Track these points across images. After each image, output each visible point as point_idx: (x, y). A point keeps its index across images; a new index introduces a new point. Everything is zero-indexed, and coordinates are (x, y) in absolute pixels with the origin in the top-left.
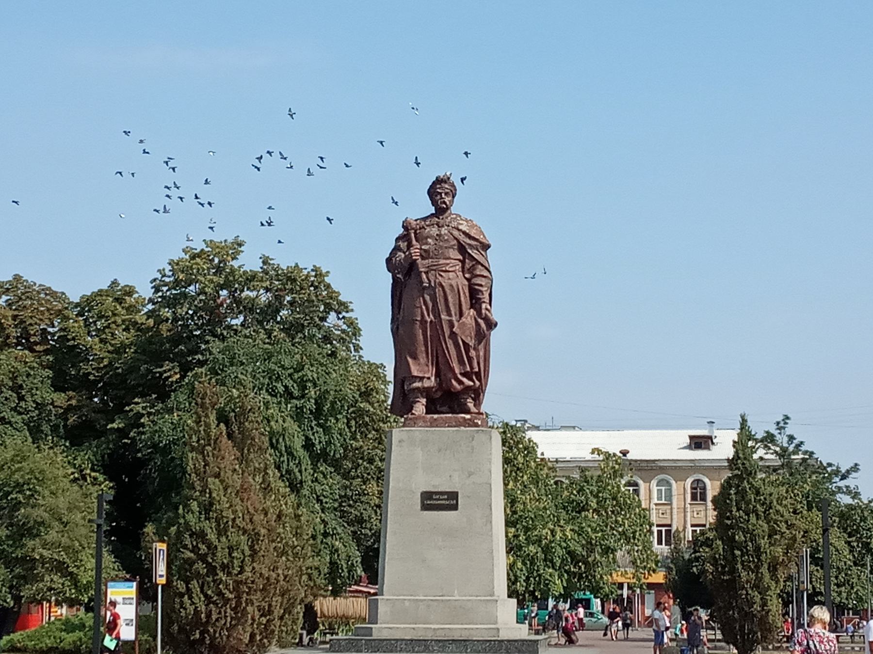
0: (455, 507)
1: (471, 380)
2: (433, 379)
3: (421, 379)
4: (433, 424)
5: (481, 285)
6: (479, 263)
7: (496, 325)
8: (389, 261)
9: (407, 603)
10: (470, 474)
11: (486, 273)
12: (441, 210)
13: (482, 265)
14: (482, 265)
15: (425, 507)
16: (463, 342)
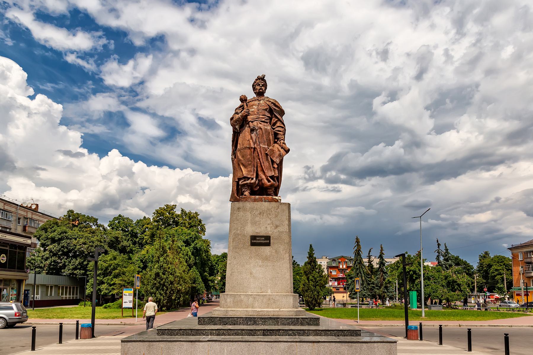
0: (268, 244)
1: (274, 180)
2: (254, 179)
3: (249, 178)
4: (255, 200)
5: (280, 131)
6: (279, 120)
7: (289, 150)
8: (232, 119)
9: (242, 297)
10: (277, 227)
11: (283, 126)
12: (260, 94)
13: (281, 122)
14: (281, 122)
15: (253, 244)
16: (271, 159)
